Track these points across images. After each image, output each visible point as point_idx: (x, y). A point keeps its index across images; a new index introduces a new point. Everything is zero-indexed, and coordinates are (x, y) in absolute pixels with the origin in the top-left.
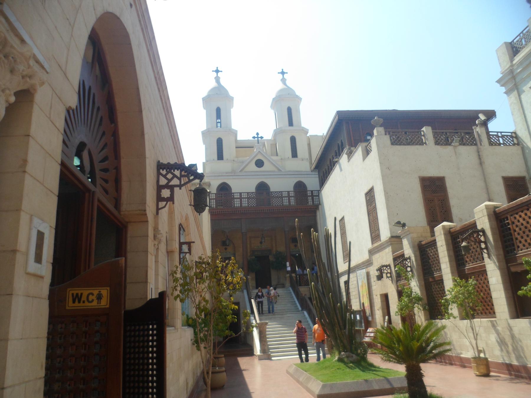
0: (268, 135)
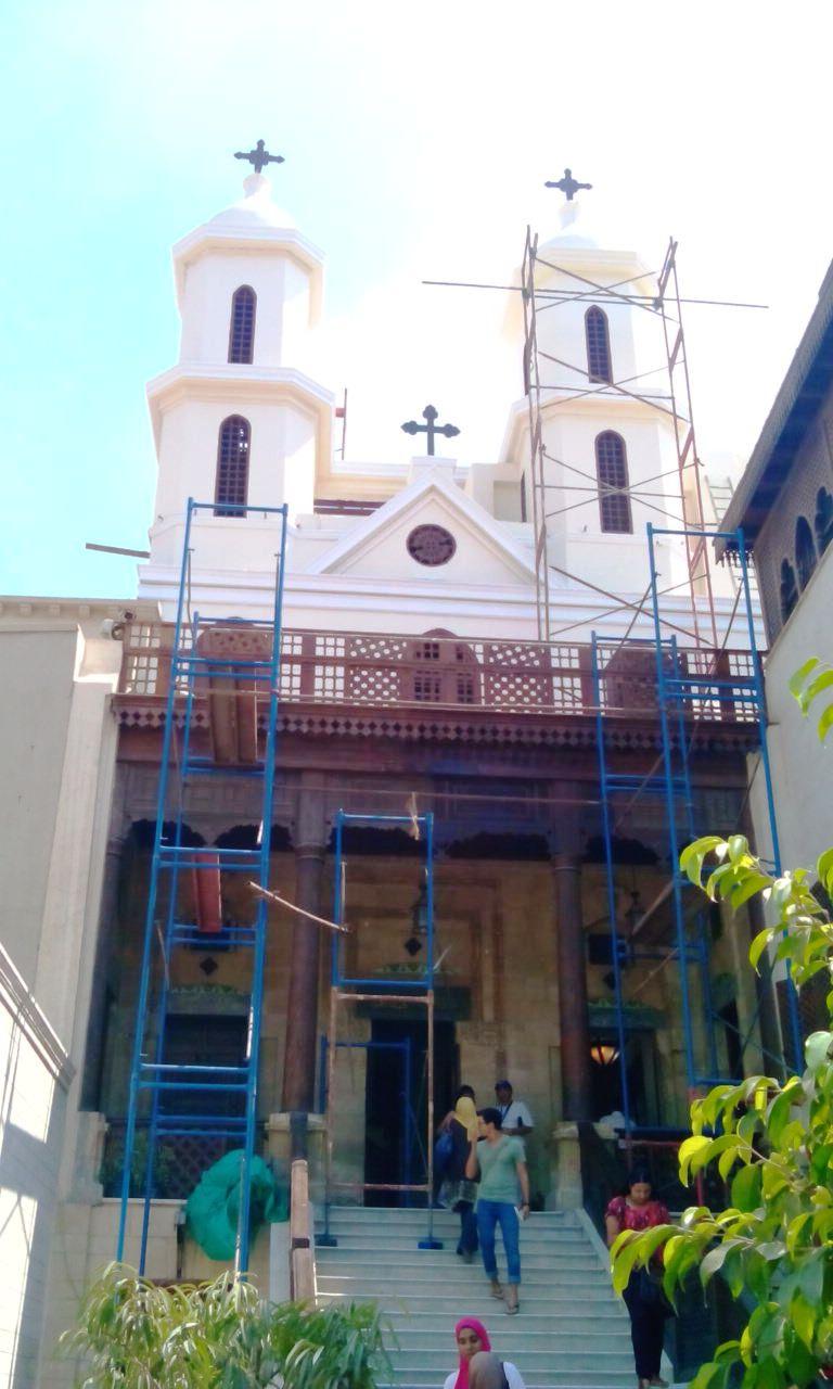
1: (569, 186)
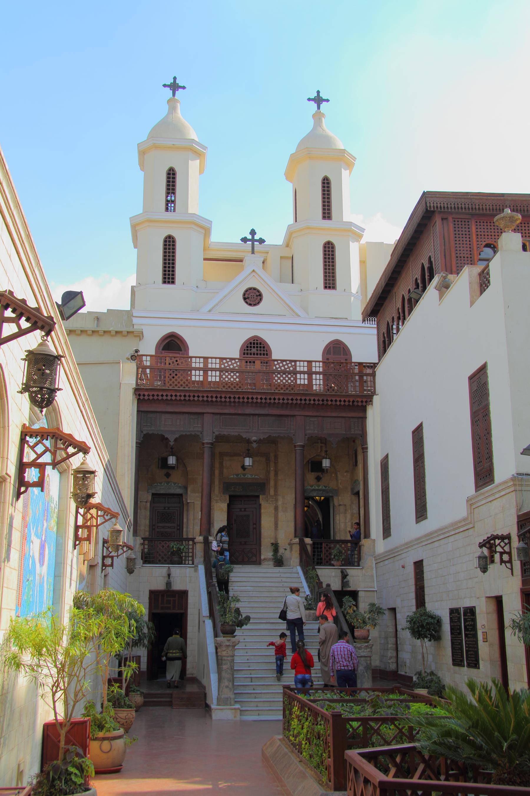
0: (274, 235)
1: (318, 100)
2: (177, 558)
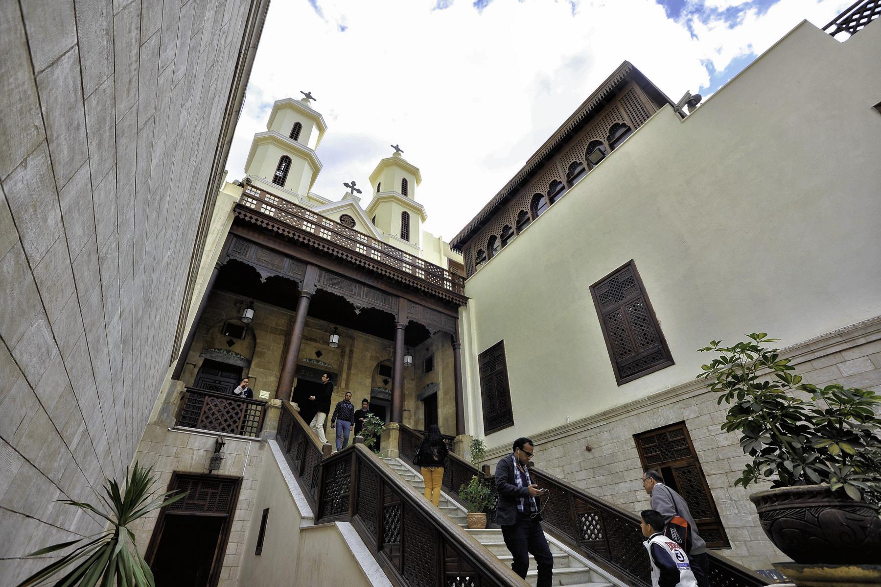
2: (238, 419)
